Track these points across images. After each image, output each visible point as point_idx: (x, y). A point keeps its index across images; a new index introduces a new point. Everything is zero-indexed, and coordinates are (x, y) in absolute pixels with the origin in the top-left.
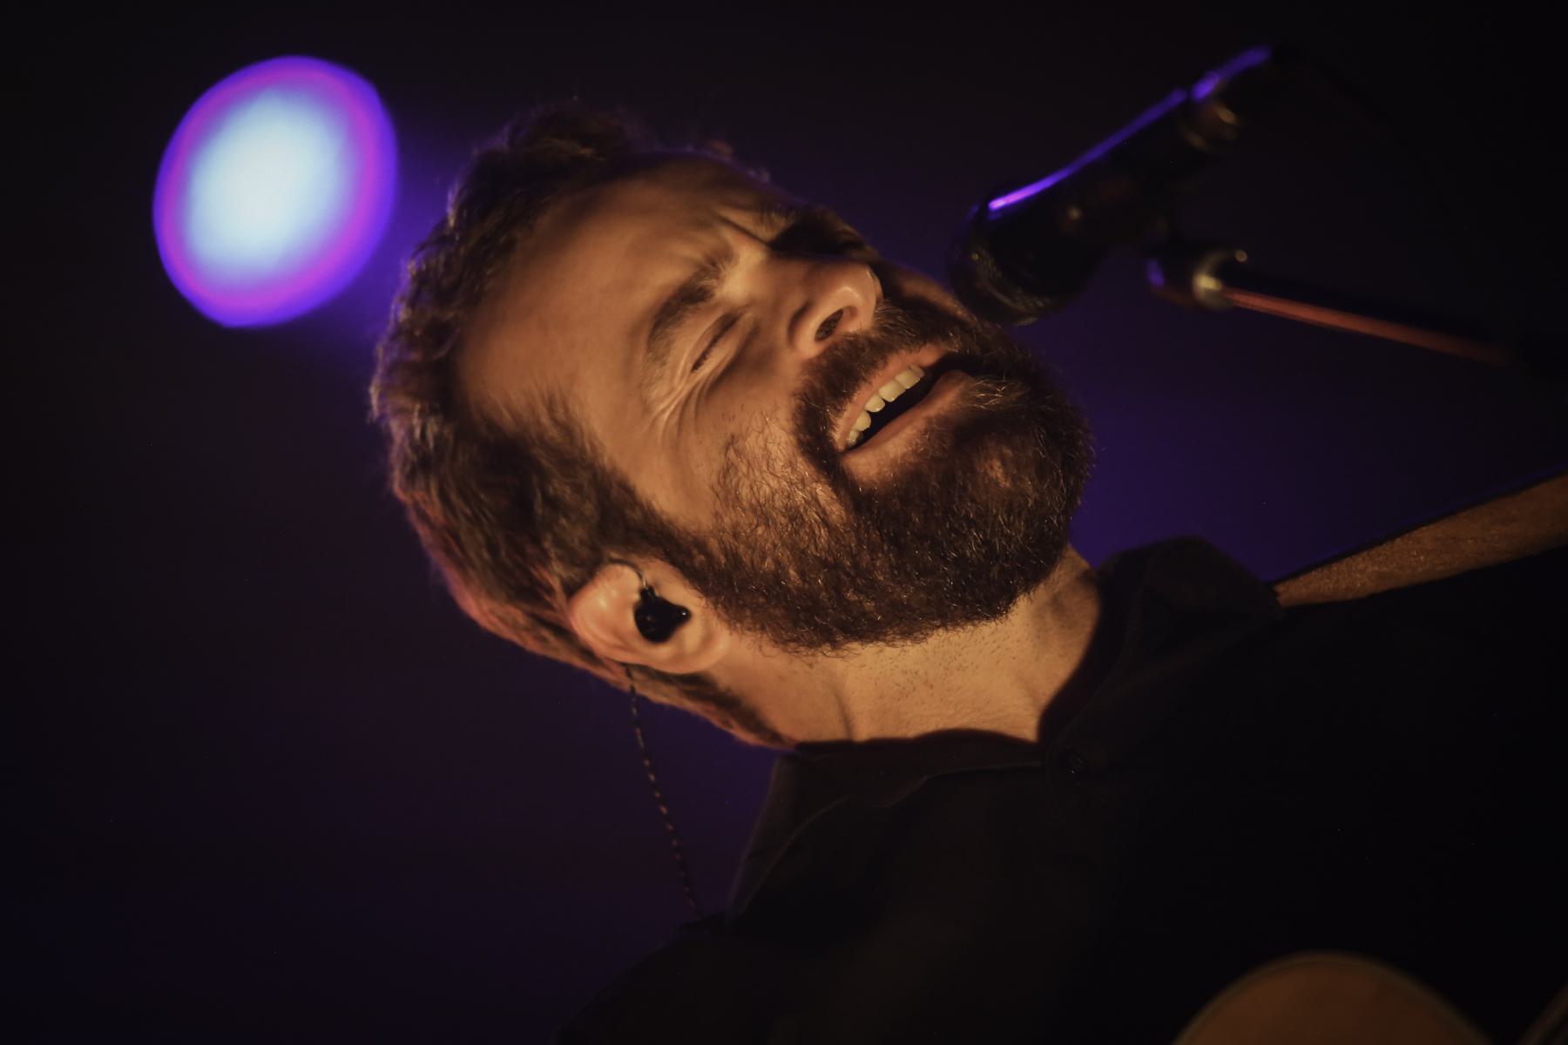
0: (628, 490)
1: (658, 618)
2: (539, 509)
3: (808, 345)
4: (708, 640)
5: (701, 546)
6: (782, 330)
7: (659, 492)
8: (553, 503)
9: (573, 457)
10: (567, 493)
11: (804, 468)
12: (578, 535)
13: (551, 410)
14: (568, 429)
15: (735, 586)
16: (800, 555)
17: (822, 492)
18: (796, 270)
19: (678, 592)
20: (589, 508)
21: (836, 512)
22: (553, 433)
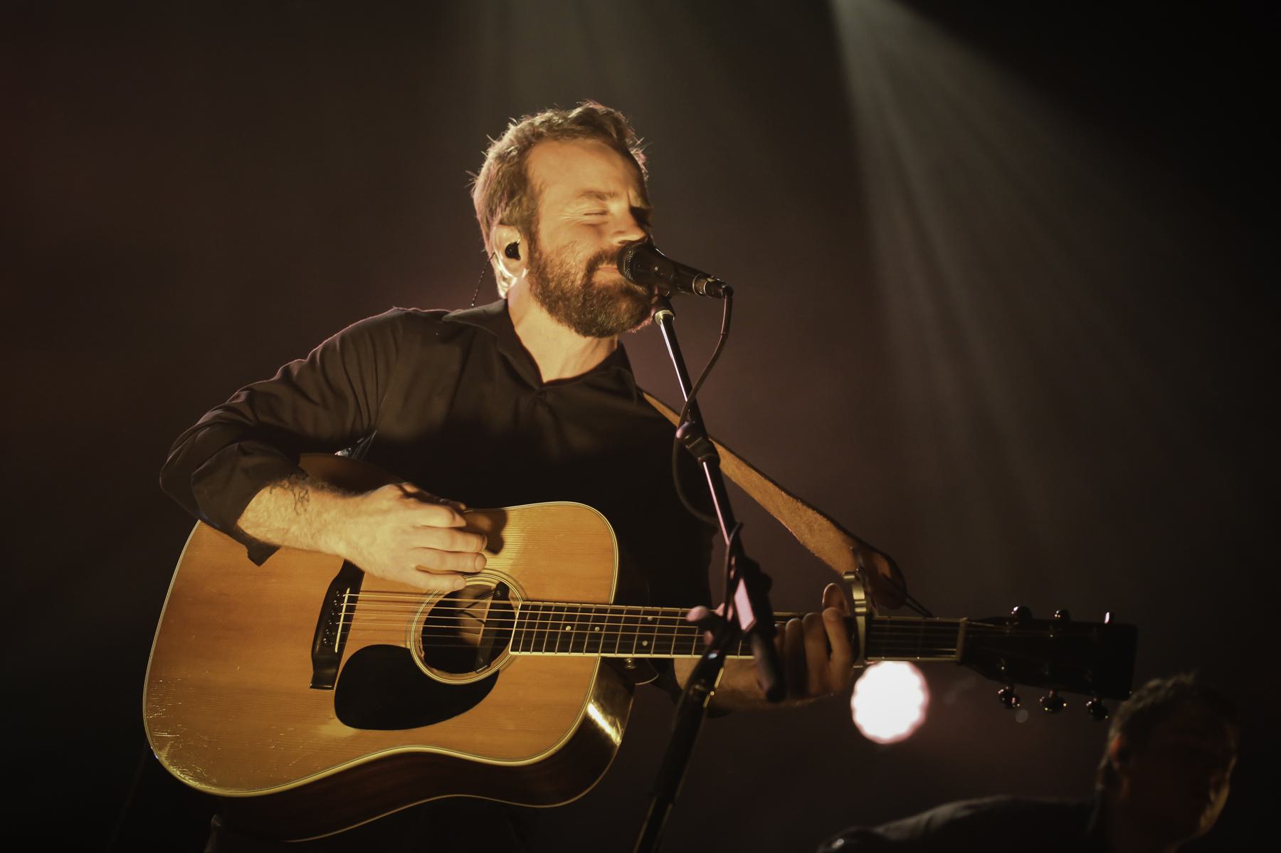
1: (512, 252)
2: (516, 199)
3: (616, 242)
5: (541, 254)
6: (613, 231)
8: (520, 200)
9: (534, 198)
11: (583, 266)
12: (516, 215)
14: (541, 192)
16: (559, 283)
18: (630, 220)
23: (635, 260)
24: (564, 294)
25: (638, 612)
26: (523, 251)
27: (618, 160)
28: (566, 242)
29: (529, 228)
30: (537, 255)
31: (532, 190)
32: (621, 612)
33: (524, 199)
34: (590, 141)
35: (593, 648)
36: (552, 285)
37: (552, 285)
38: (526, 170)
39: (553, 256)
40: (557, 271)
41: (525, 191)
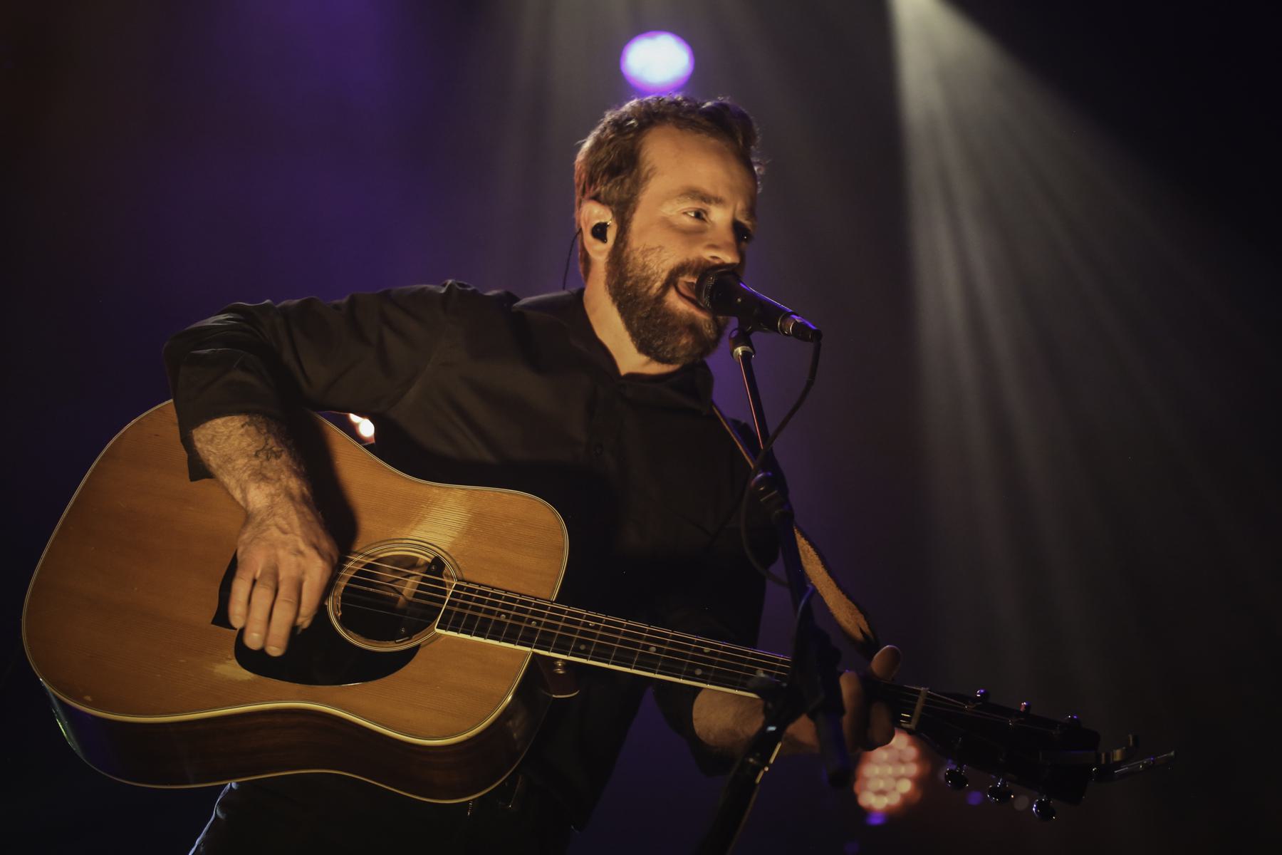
0: (634, 210)
1: (600, 232)
4: (600, 253)
5: (625, 246)
7: (639, 220)
8: (622, 181)
9: (638, 183)
10: (627, 186)
12: (615, 194)
13: (650, 170)
14: (647, 179)
15: (618, 259)
17: (658, 284)
19: (611, 235)
20: (625, 196)
21: (654, 291)
22: (643, 175)
23: (715, 286)
24: (636, 297)
25: (580, 616)
26: (611, 235)
27: (736, 169)
28: (655, 245)
29: (624, 211)
30: (621, 245)
31: (639, 173)
32: (562, 612)
33: (628, 181)
34: (713, 141)
35: (526, 641)
36: (629, 283)
37: (629, 283)
38: (639, 151)
39: (637, 254)
40: (637, 272)
41: (631, 172)
